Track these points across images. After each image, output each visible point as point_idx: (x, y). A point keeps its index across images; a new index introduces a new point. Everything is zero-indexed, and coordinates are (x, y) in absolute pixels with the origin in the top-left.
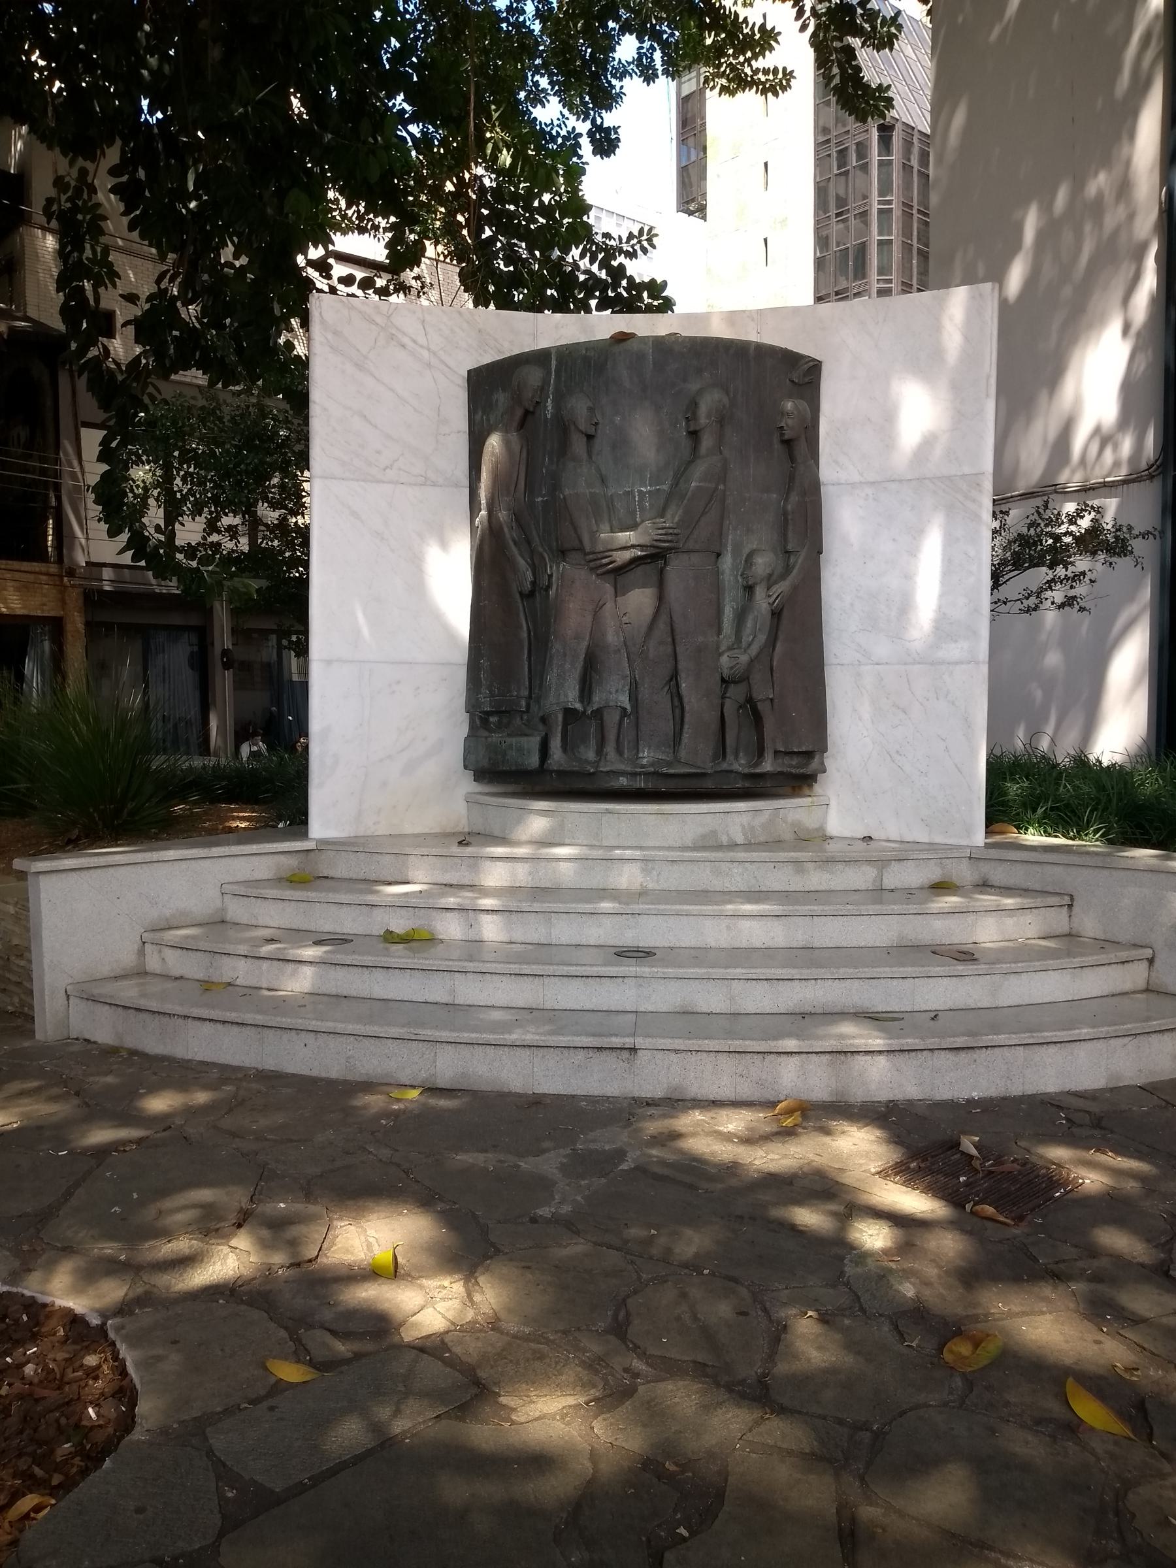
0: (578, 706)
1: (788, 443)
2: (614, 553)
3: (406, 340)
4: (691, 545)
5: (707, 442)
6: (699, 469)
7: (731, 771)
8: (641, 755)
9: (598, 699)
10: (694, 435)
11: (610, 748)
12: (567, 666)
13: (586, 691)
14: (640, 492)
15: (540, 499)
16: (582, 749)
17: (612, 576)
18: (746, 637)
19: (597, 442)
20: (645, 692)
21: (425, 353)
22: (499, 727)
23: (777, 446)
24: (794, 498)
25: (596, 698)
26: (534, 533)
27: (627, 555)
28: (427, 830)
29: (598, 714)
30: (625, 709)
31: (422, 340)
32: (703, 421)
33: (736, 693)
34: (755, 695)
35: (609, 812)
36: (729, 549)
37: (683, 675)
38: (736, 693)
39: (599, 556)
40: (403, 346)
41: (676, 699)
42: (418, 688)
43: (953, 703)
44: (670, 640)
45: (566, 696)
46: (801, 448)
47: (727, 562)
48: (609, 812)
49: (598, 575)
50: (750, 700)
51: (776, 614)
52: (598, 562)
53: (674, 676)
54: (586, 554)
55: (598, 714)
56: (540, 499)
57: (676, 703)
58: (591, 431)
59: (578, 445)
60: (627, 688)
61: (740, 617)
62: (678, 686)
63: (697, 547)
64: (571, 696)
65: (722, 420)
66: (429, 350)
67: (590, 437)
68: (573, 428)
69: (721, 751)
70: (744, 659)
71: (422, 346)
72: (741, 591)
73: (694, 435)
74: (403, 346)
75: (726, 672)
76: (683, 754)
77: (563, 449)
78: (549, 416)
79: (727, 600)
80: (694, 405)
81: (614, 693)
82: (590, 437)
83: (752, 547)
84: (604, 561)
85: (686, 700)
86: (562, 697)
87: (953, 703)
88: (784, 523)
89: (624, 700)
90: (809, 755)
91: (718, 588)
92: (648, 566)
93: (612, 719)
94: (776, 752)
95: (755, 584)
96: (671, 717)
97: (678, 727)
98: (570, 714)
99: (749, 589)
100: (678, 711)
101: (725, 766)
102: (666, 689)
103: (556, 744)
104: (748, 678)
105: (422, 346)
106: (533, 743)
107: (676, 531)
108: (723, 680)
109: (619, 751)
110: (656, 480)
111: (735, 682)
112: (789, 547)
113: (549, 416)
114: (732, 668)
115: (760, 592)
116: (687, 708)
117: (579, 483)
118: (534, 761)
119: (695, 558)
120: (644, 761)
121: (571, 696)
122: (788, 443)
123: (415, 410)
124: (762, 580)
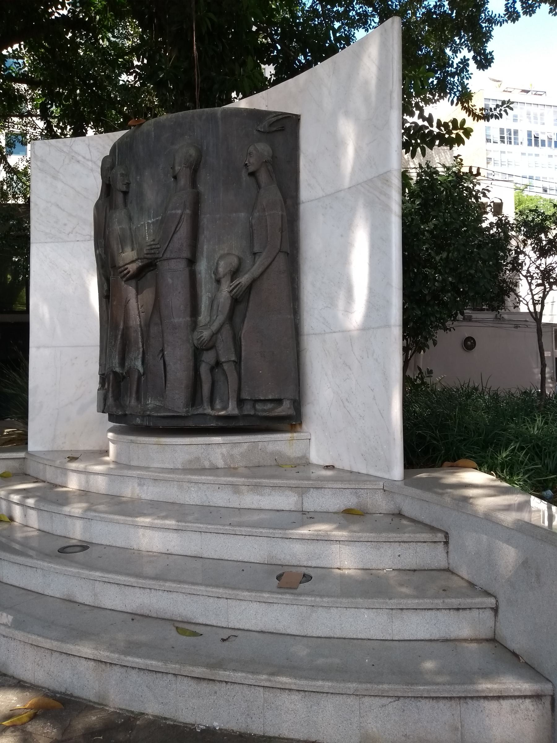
0: (118, 370)
3: (80, 158)
7: (205, 414)
14: (148, 223)
21: (90, 164)
24: (256, 214)
28: (91, 448)
31: (88, 157)
35: (132, 442)
36: (205, 254)
39: (123, 269)
40: (78, 162)
42: (87, 361)
43: (377, 360)
48: (132, 442)
58: (124, 188)
66: (91, 161)
67: (125, 193)
71: (88, 160)
74: (78, 162)
79: (204, 291)
82: (125, 193)
84: (125, 272)
87: (377, 360)
101: (200, 411)
105: (88, 160)
112: (256, 250)
123: (85, 197)
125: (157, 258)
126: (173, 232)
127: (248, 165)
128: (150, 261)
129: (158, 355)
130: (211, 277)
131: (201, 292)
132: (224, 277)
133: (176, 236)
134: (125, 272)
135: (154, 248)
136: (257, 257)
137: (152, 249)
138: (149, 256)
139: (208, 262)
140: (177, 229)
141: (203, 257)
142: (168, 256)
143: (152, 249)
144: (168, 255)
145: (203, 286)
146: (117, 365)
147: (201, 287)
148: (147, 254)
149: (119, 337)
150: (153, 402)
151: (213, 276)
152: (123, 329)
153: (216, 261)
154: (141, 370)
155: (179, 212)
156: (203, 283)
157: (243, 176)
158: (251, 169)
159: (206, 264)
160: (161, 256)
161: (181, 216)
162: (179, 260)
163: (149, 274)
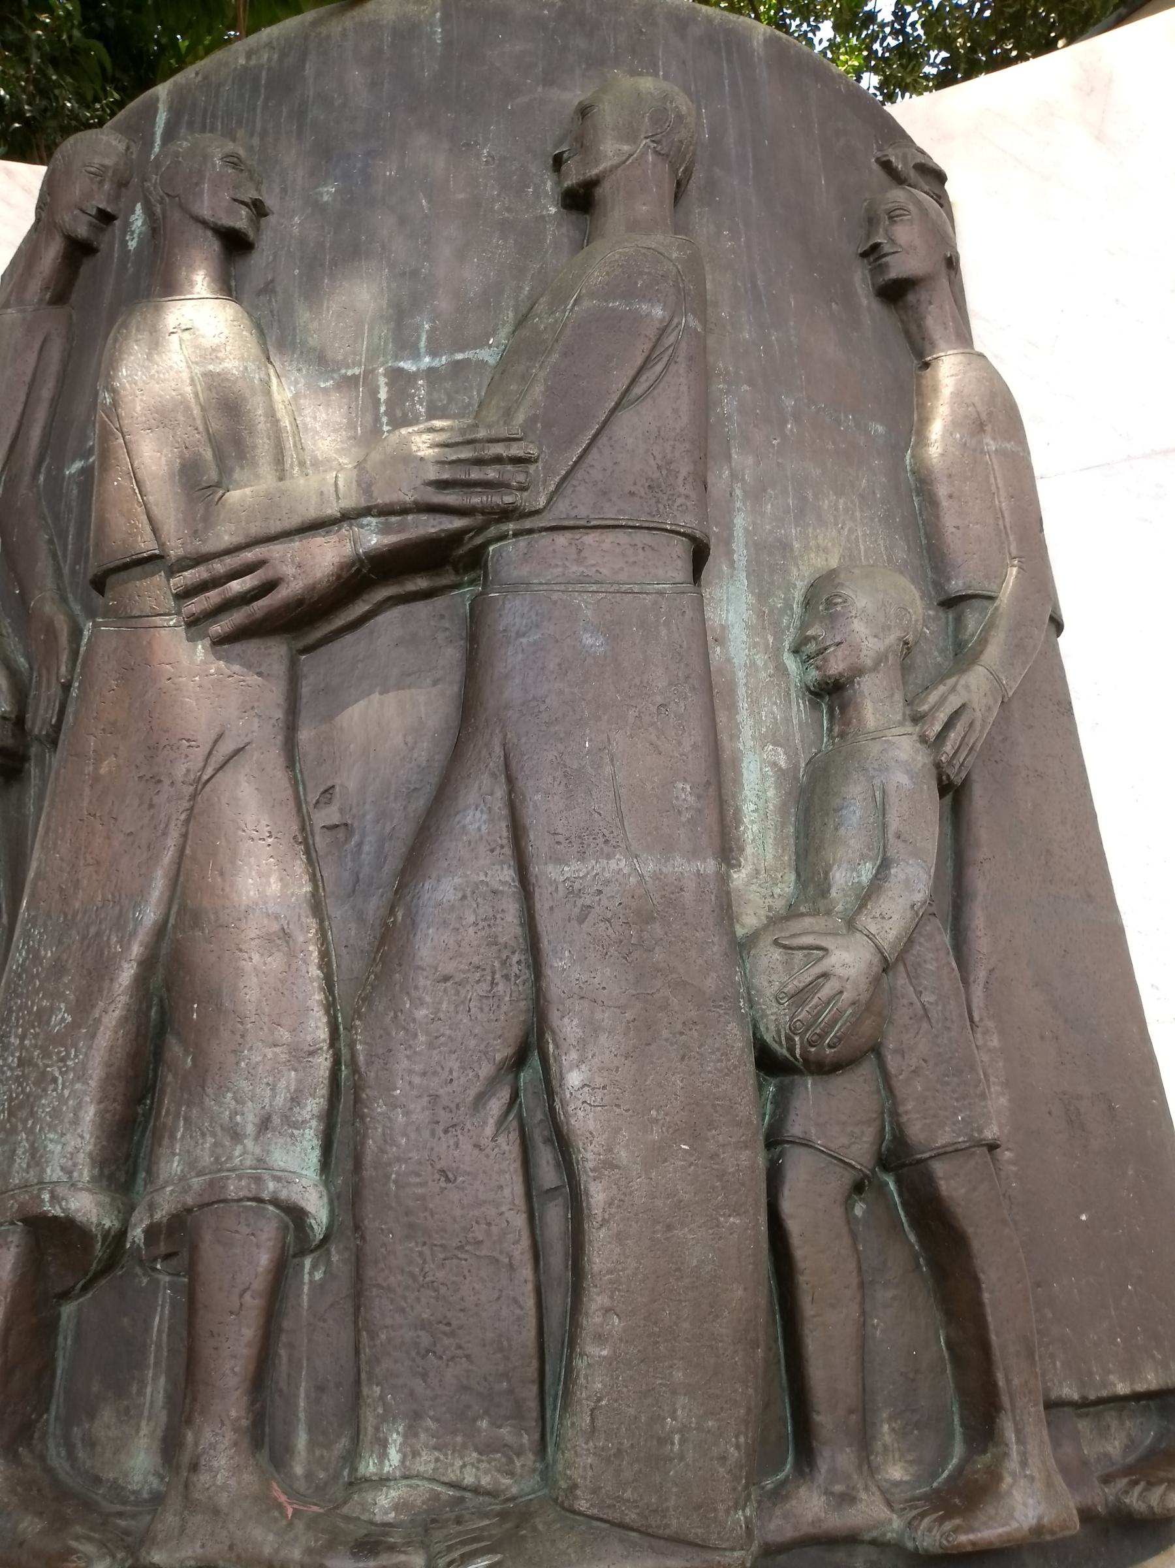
0: (86, 1206)
1: (895, 293)
2: (275, 551)
4: (579, 503)
7: (850, 1540)
8: (369, 1466)
9: (177, 1171)
12: (62, 1017)
15: (78, 465)
16: (106, 1421)
17: (276, 652)
18: (847, 875)
19: (260, 259)
23: (865, 298)
25: (172, 1166)
26: (44, 565)
27: (325, 556)
29: (179, 1236)
30: (296, 1214)
32: (611, 149)
33: (834, 1119)
34: (916, 1131)
37: (567, 1027)
38: (834, 1119)
39: (219, 567)
41: (545, 1158)
44: (507, 874)
45: (37, 1157)
47: (732, 604)
49: (220, 642)
50: (898, 1157)
52: (213, 597)
53: (531, 1049)
54: (171, 572)
56: (78, 465)
57: (548, 1174)
58: (240, 220)
60: (314, 1105)
61: (810, 803)
62: (549, 1087)
63: (610, 513)
68: (176, 216)
69: (793, 1428)
70: (849, 961)
72: (799, 710)
75: (775, 1021)
76: (580, 1459)
78: (132, 245)
79: (747, 733)
85: (589, 1155)
86: (21, 1162)
89: (297, 1168)
92: (421, 609)
94: (1052, 1405)
95: (858, 671)
96: (521, 1250)
97: (557, 1302)
100: (555, 1217)
101: (811, 1508)
102: (496, 1106)
104: (876, 1049)
107: (516, 450)
108: (768, 1062)
109: (263, 1435)
110: (454, 335)
111: (824, 1069)
113: (132, 245)
114: (800, 996)
116: (598, 1195)
119: (604, 554)
120: (384, 1504)
124: (881, 658)
125: (506, 514)
126: (615, 397)
127: (887, 248)
128: (457, 523)
129: (481, 1099)
130: (782, 669)
131: (734, 737)
132: (875, 668)
133: (626, 417)
134: (236, 586)
135: (498, 460)
136: (973, 621)
137: (479, 462)
138: (450, 498)
139: (762, 592)
140: (637, 390)
141: (732, 564)
142: (583, 511)
143: (479, 462)
144: (579, 503)
145: (743, 705)
146: (85, 1174)
147: (732, 708)
148: (442, 485)
149: (127, 974)
150: (425, 1463)
151: (791, 664)
152: (161, 930)
153: (798, 595)
154: (317, 1207)
155: (658, 312)
156: (741, 691)
157: (860, 291)
158: (899, 267)
159: (751, 599)
160: (542, 501)
161: (663, 331)
162: (643, 538)
163: (394, 614)
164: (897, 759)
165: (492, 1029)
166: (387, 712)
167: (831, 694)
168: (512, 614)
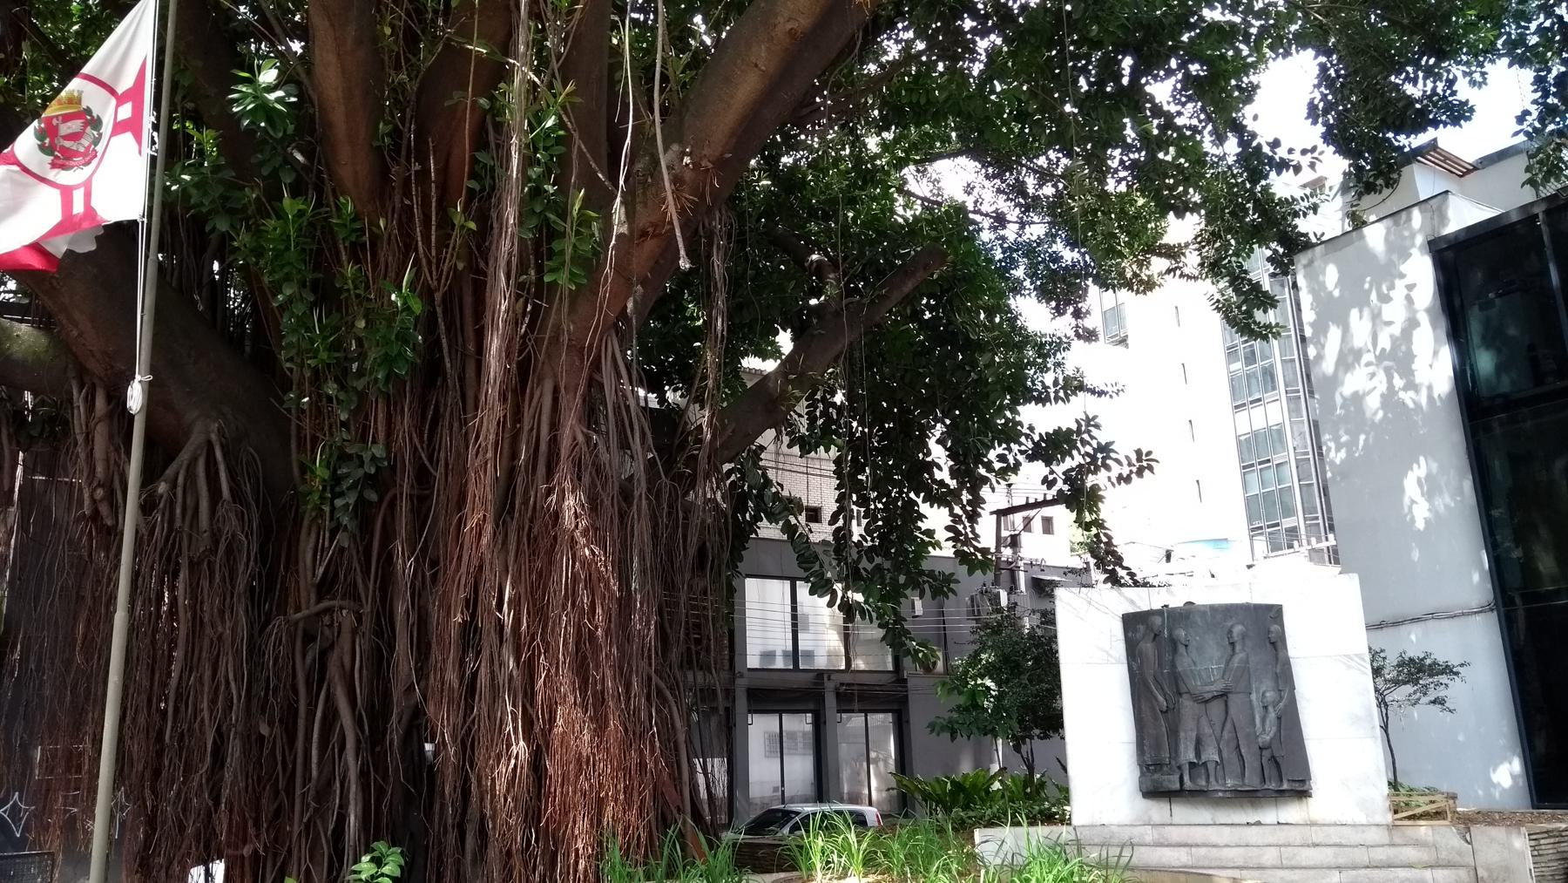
1: (1273, 644)
5: (1238, 647)
6: (1237, 659)
10: (1233, 644)
11: (1212, 779)
13: (1198, 754)
20: (1225, 755)
22: (1155, 771)
33: (1266, 754)
38: (1266, 754)
46: (1279, 644)
47: (1253, 696)
51: (1279, 718)
53: (1238, 746)
55: (1205, 764)
59: (1182, 649)
61: (1263, 720)
64: (1191, 756)
65: (1244, 636)
69: (1264, 780)
73: (1233, 644)
77: (1175, 650)
80: (1230, 632)
81: (1210, 755)
83: (1263, 690)
88: (1276, 677)
90: (1303, 781)
91: (1252, 708)
93: (1211, 767)
98: (1192, 764)
99: (1265, 708)
103: (1186, 778)
106: (1176, 777)
115: (1271, 709)
117: (1184, 663)
118: (1177, 786)
121: (1191, 756)
122: (1273, 644)
164: (1272, 715)
165: (1233, 745)
166: (1216, 708)
167: (1265, 708)
168: (1231, 704)
